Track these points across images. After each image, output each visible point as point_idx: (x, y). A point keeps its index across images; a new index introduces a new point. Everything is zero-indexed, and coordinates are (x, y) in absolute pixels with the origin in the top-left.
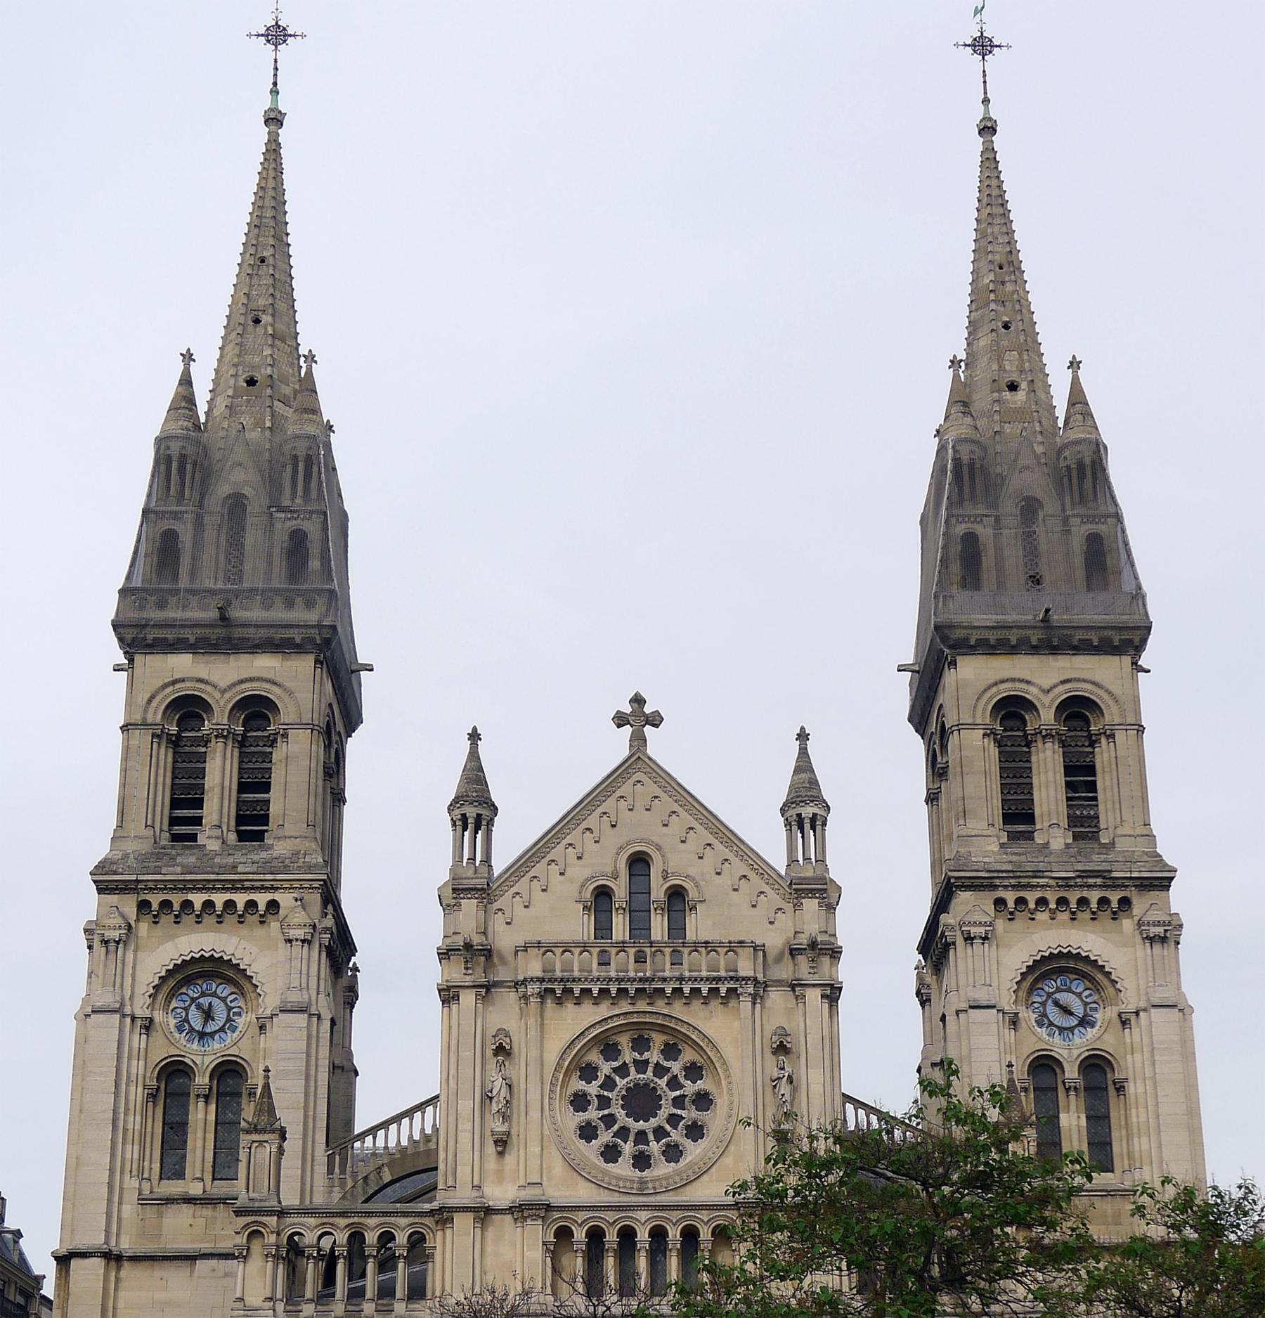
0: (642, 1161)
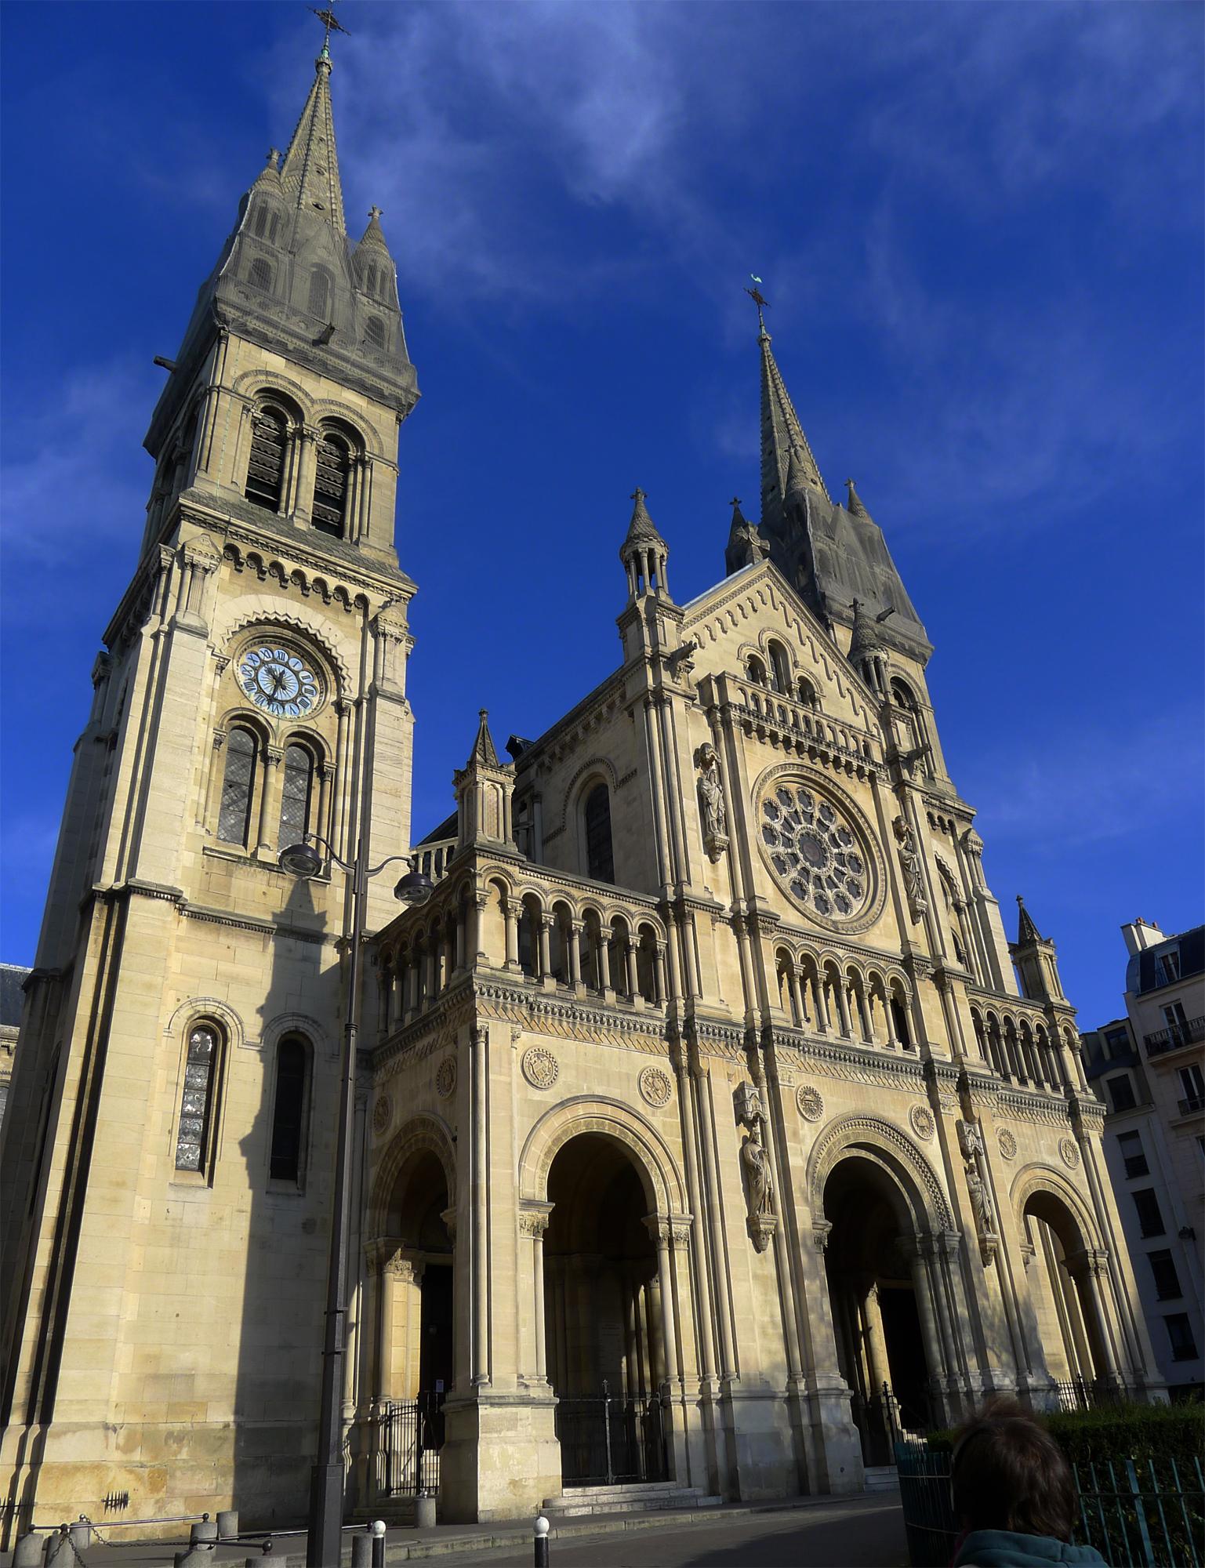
0: (822, 903)
